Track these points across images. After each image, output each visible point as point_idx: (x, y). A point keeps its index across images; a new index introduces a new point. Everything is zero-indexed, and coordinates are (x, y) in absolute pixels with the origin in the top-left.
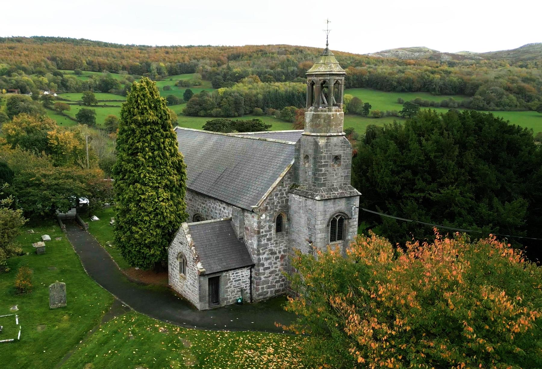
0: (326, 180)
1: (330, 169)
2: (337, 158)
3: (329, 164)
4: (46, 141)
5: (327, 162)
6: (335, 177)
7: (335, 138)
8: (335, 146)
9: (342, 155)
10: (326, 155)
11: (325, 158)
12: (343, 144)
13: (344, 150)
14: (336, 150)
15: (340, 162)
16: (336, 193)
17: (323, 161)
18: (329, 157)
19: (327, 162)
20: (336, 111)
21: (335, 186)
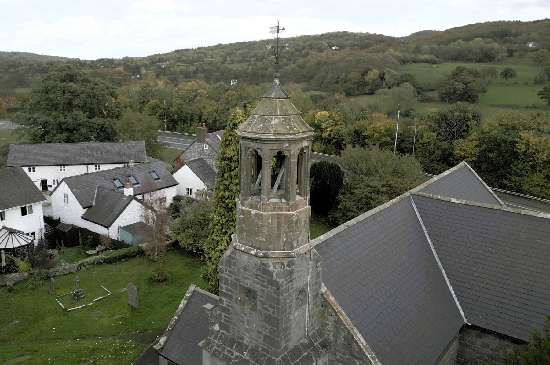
0: (230, 323)
1: (237, 307)
2: (250, 293)
3: (234, 296)
4: (514, 143)
5: (231, 291)
6: (246, 326)
7: (245, 257)
8: (245, 269)
9: (259, 293)
10: (229, 278)
11: (226, 283)
12: (260, 273)
13: (264, 286)
14: (246, 278)
15: (255, 304)
16: (236, 353)
17: (224, 286)
18: (235, 285)
19: (231, 291)
20: (251, 206)
21: (245, 342)
